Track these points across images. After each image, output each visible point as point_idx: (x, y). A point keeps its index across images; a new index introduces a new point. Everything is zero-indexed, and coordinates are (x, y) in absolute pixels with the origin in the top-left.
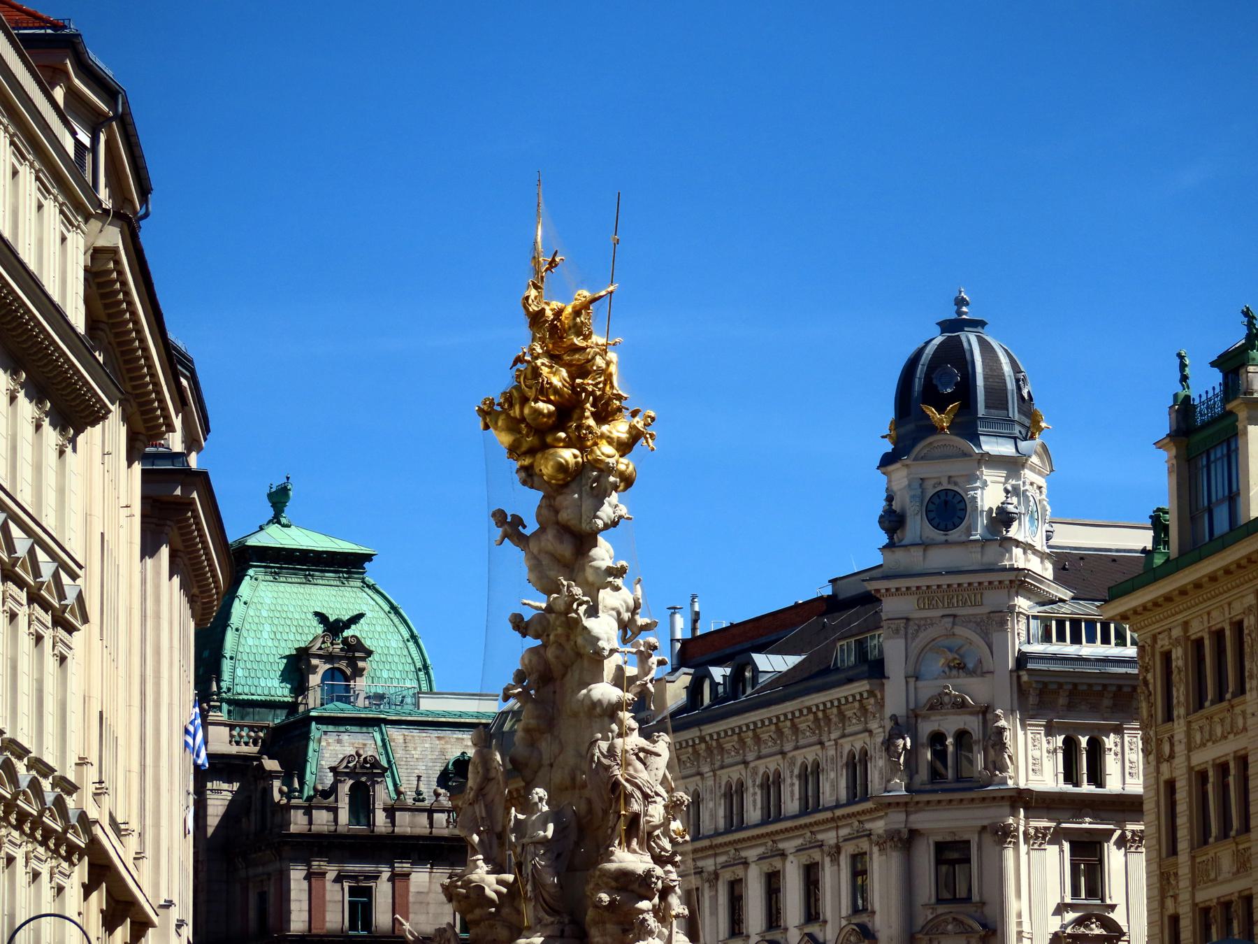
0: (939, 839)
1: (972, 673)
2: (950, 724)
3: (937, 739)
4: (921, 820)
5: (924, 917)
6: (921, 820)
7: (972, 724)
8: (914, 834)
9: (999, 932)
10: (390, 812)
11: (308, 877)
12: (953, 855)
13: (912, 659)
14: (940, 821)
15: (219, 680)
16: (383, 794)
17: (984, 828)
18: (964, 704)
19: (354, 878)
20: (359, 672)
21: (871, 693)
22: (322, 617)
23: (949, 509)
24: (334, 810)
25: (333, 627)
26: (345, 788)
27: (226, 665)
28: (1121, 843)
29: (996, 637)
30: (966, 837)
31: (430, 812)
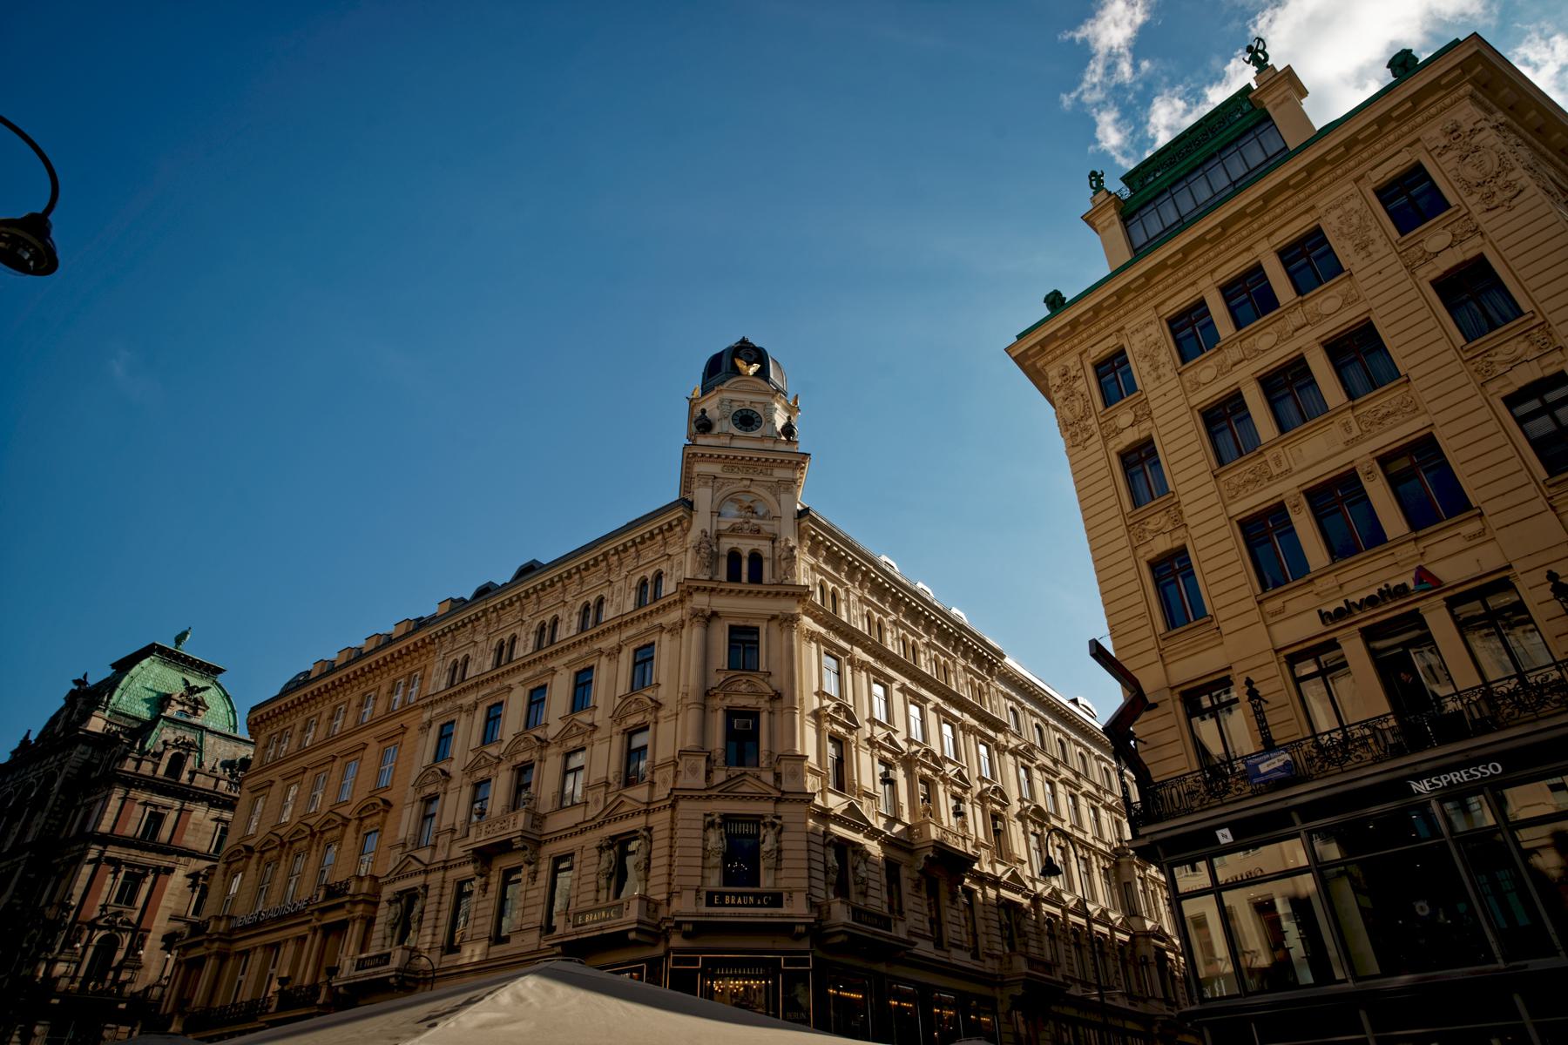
0: (733, 622)
1: (763, 518)
2: (745, 546)
3: (734, 557)
4: (720, 603)
5: (716, 680)
6: (720, 603)
7: (764, 547)
8: (715, 614)
9: (786, 698)
10: (193, 773)
11: (124, 799)
12: (744, 641)
13: (717, 501)
14: (740, 606)
15: (110, 697)
16: (191, 763)
17: (774, 618)
18: (758, 531)
19: (156, 806)
20: (195, 713)
21: (680, 520)
22: (187, 683)
23: (747, 420)
24: (156, 766)
25: (191, 690)
26: (168, 755)
27: (117, 693)
28: (851, 662)
29: (784, 497)
30: (755, 624)
31: (218, 779)
